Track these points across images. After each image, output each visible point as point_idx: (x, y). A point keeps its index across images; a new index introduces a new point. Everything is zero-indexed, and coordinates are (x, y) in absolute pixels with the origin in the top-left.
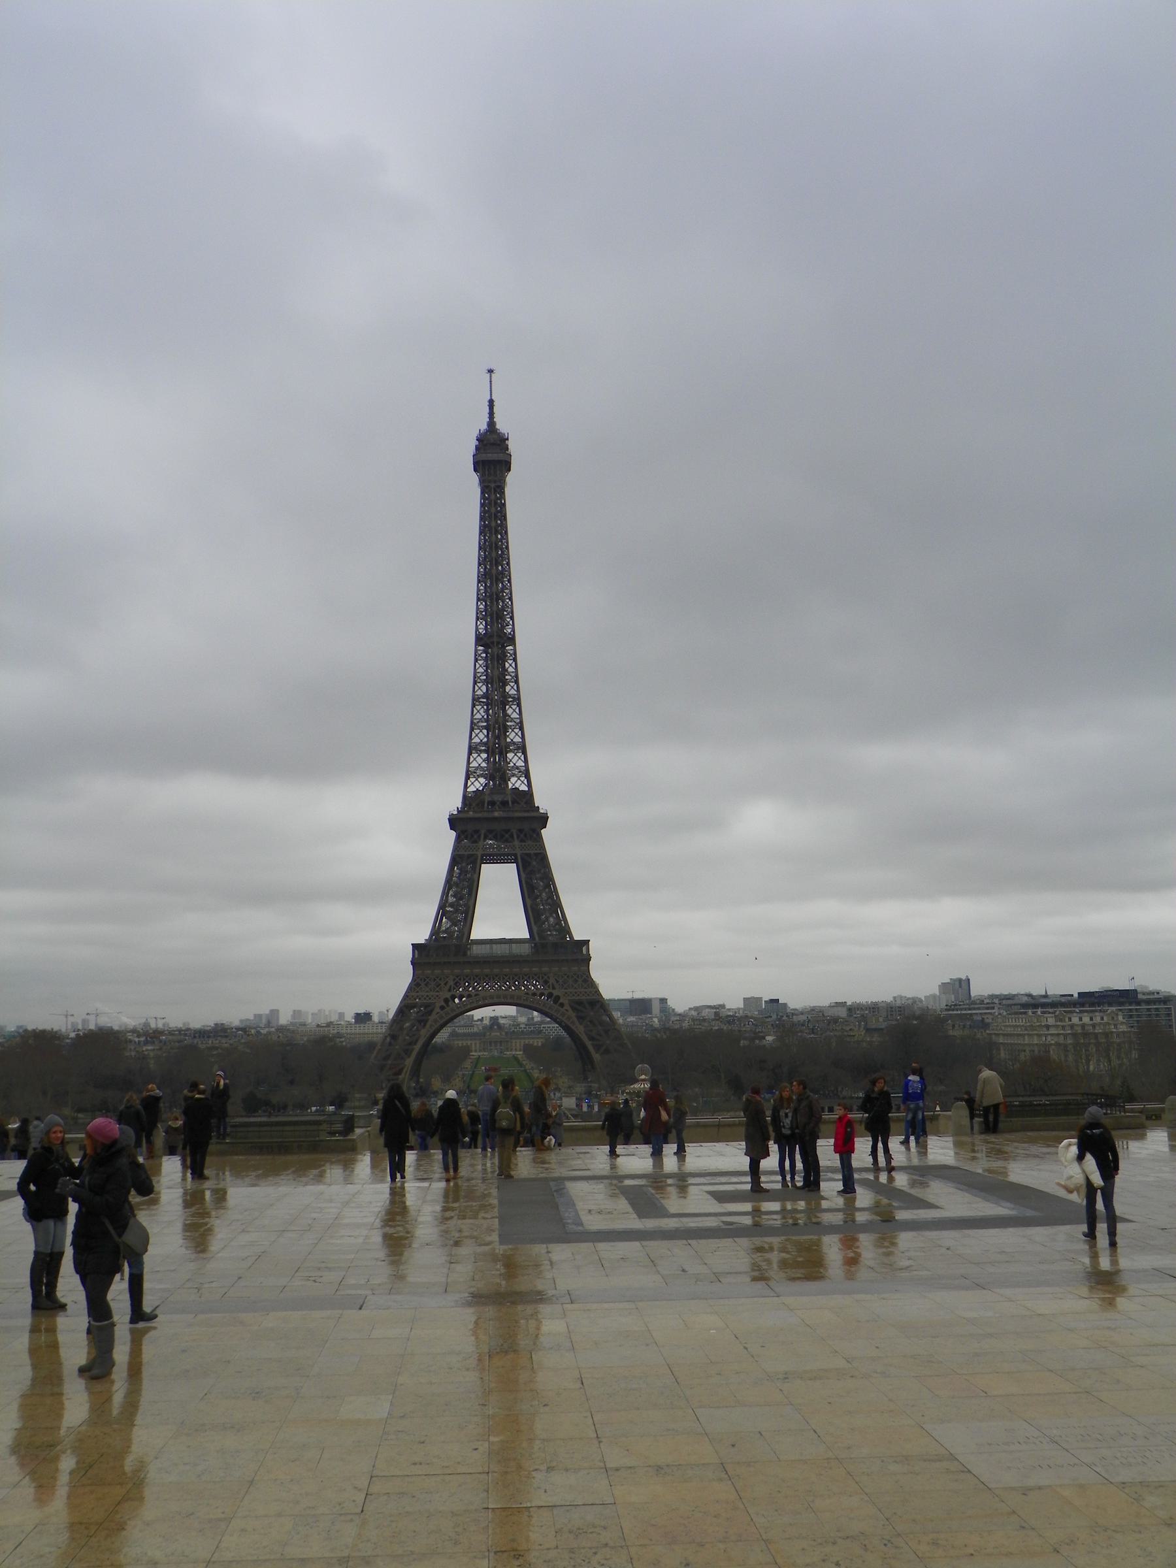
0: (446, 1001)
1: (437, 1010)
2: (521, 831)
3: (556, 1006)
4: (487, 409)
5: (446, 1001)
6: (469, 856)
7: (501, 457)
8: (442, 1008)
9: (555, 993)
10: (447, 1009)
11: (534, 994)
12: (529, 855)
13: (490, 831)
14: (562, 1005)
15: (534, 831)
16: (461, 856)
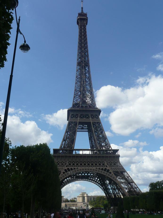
0: (65, 170)
1: (62, 173)
2: (92, 115)
3: (108, 173)
4: (81, 9)
5: (65, 170)
6: (75, 122)
7: (85, 17)
8: (64, 173)
9: (107, 168)
10: (66, 173)
11: (99, 169)
12: (95, 122)
13: (81, 115)
14: (110, 173)
15: (97, 115)
16: (72, 122)
